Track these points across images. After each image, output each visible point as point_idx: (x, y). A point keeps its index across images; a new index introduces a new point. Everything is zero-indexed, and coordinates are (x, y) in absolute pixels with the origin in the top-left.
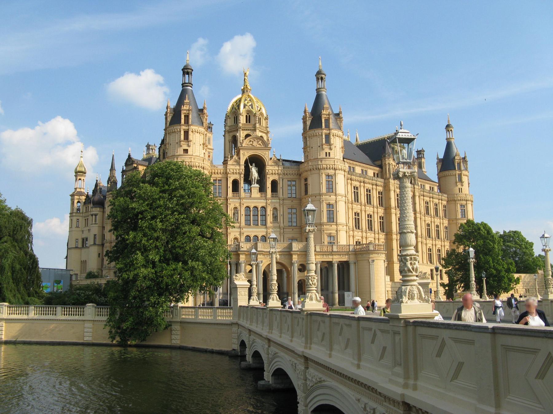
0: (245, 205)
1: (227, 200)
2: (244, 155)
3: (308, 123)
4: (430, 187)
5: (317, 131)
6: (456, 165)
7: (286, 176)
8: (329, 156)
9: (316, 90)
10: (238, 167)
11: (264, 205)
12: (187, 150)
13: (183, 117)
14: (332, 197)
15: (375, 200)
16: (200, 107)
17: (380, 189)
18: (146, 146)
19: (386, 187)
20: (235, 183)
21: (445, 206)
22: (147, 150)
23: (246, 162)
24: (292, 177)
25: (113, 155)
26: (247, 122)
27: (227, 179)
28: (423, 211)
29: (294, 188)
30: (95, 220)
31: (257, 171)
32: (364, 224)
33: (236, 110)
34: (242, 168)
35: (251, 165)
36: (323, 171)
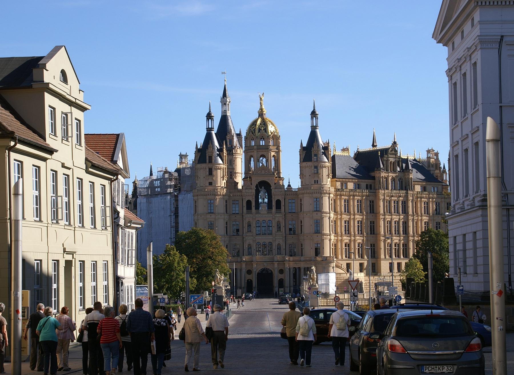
1: (243, 216)
2: (256, 180)
3: (303, 157)
5: (309, 164)
7: (288, 196)
8: (317, 183)
9: (311, 127)
10: (250, 191)
12: (212, 182)
13: (207, 158)
18: (179, 155)
20: (249, 203)
22: (180, 159)
23: (257, 186)
25: (151, 166)
27: (243, 200)
29: (293, 205)
35: (261, 188)
36: (311, 195)
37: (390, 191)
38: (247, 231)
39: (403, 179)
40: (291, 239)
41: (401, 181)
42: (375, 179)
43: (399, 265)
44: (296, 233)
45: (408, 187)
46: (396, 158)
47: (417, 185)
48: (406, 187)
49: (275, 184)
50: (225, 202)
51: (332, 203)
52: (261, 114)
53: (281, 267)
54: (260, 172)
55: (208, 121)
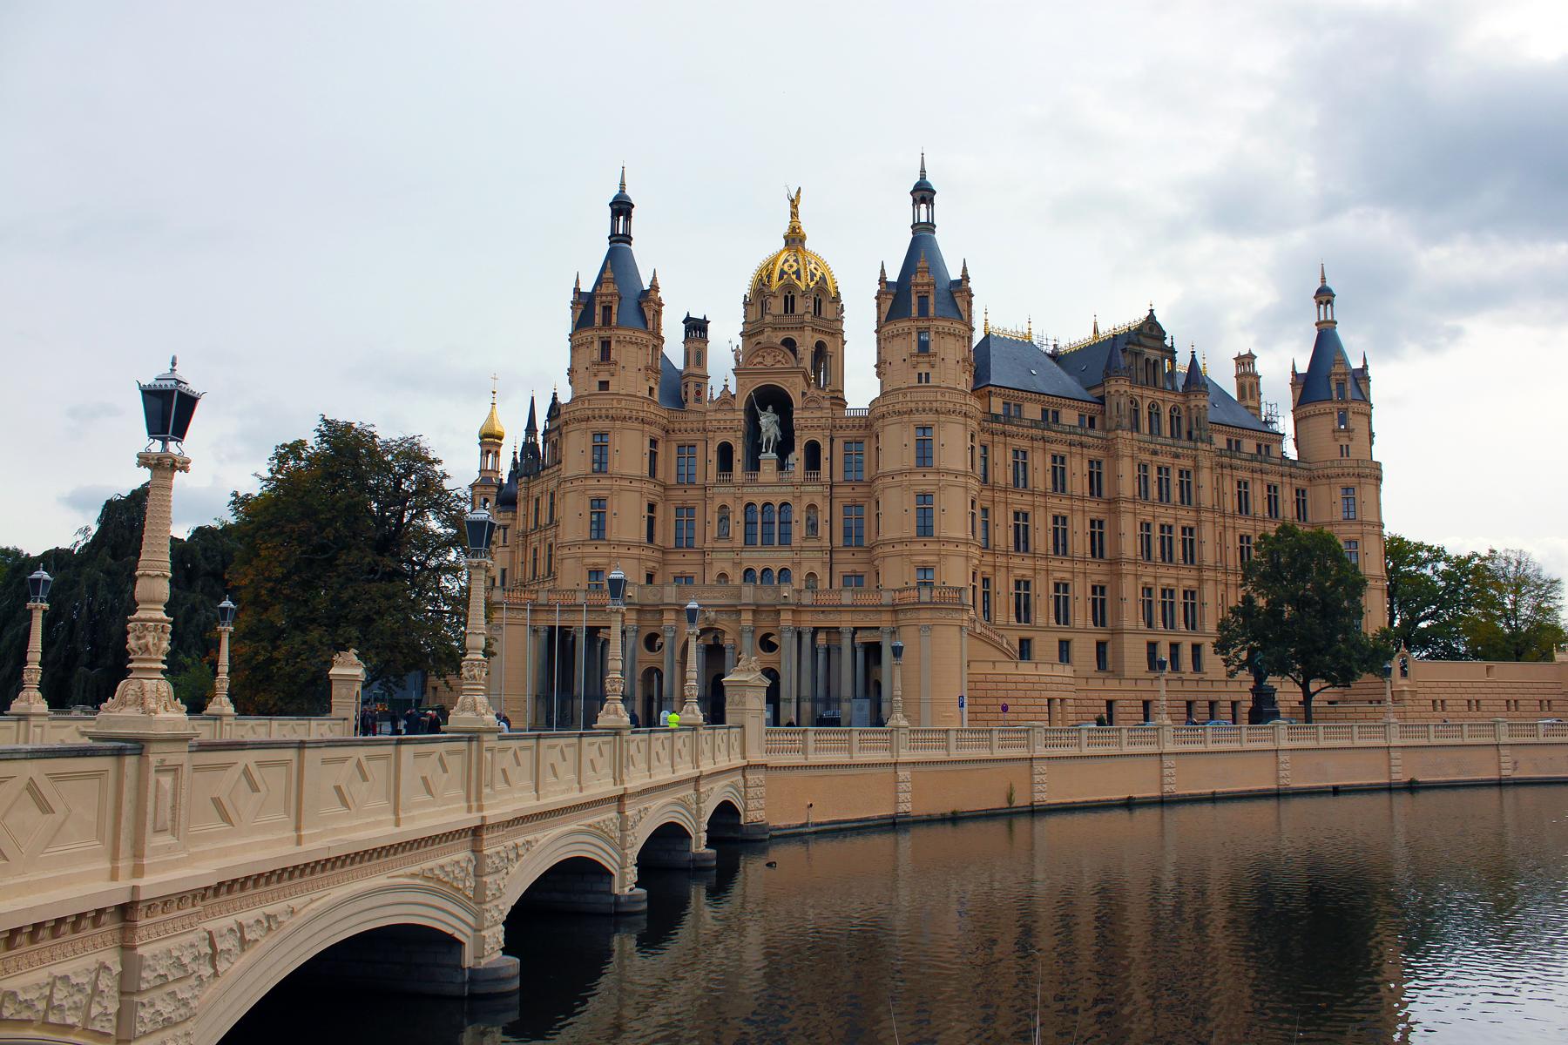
0: (747, 500)
3: (886, 307)
4: (1259, 446)
5: (903, 325)
6: (1334, 386)
7: (841, 432)
8: (927, 381)
9: (912, 227)
10: (730, 416)
11: (789, 499)
14: (929, 477)
15: (1078, 480)
16: (646, 287)
17: (1094, 453)
19: (1110, 449)
20: (725, 452)
21: (1300, 492)
23: (749, 401)
24: (854, 433)
25: (533, 398)
26: (786, 311)
28: (1231, 504)
30: (505, 538)
31: (776, 422)
32: (1041, 539)
33: (764, 285)
34: (739, 417)
35: (764, 409)
37: (1148, 438)
38: (716, 535)
39: (1183, 413)
40: (848, 563)
41: (1175, 414)
42: (1104, 404)
43: (1175, 647)
44: (866, 544)
45: (1195, 433)
46: (1161, 350)
47: (1220, 432)
48: (1190, 433)
49: (804, 394)
50: (647, 443)
51: (973, 447)
52: (794, 239)
53: (766, 625)
54: (760, 359)
55: (618, 220)
